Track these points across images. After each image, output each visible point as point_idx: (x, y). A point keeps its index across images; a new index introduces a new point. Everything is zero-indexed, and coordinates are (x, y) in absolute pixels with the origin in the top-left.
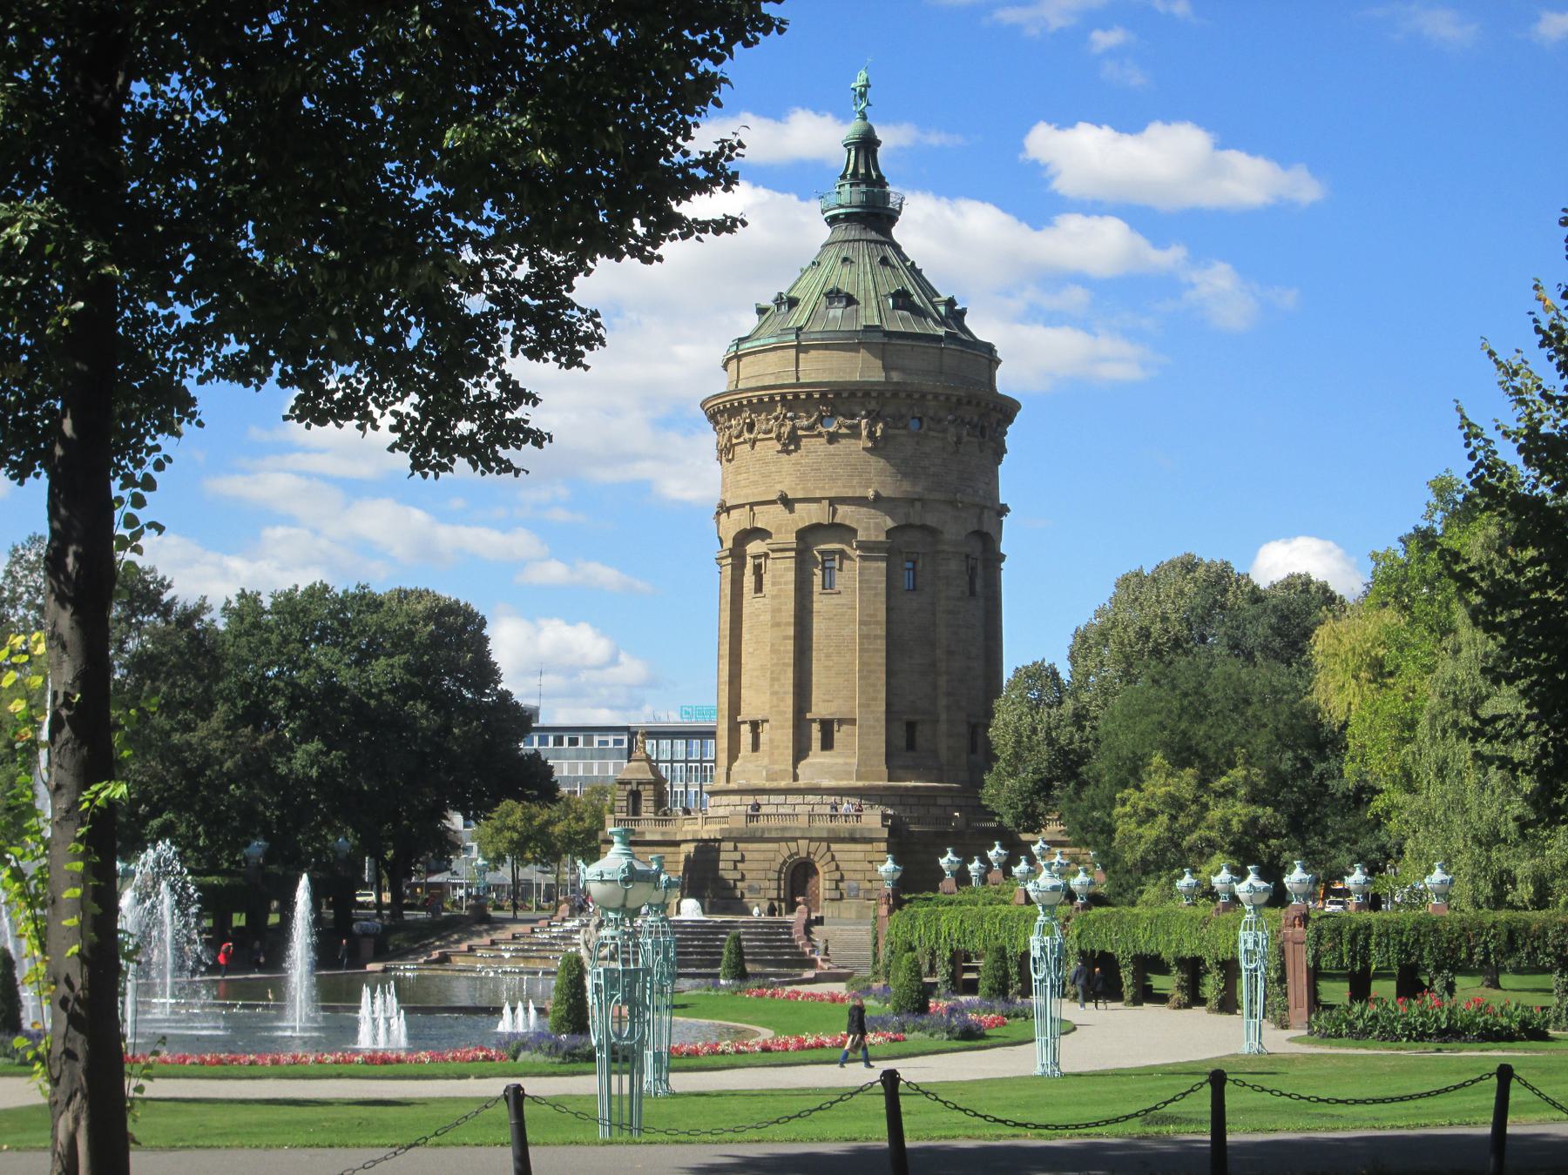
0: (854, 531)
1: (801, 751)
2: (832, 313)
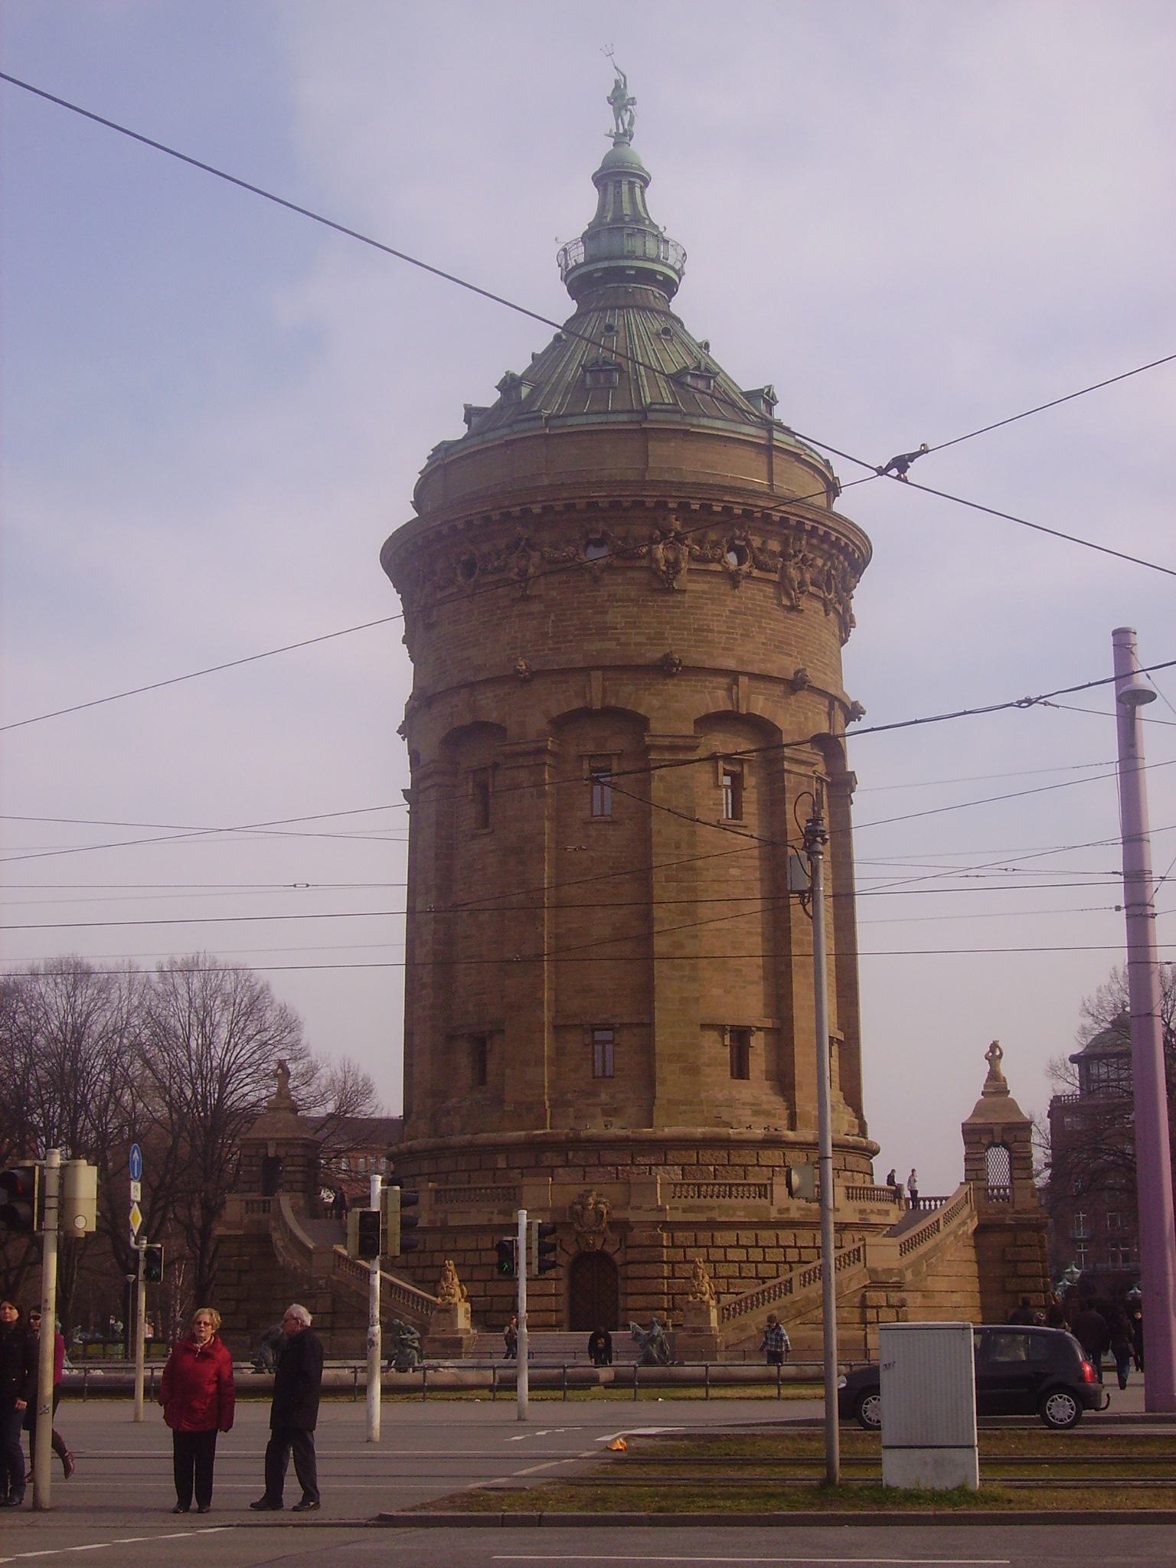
0: (640, 723)
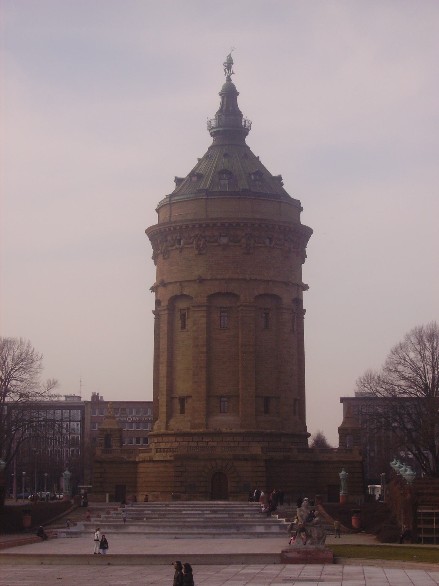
0: (237, 297)
1: (209, 413)
2: (222, 182)
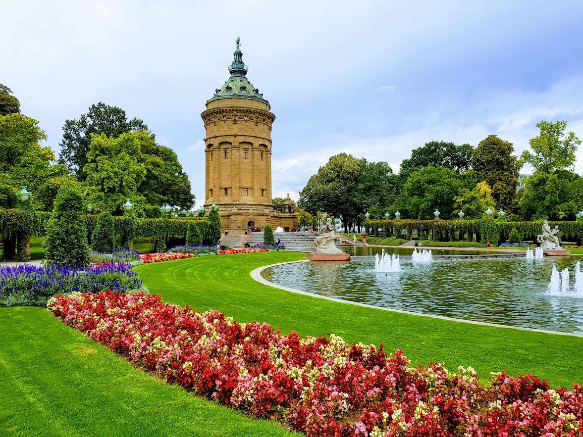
0: (252, 144)
